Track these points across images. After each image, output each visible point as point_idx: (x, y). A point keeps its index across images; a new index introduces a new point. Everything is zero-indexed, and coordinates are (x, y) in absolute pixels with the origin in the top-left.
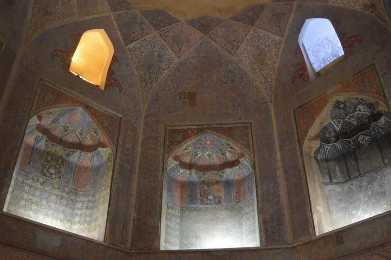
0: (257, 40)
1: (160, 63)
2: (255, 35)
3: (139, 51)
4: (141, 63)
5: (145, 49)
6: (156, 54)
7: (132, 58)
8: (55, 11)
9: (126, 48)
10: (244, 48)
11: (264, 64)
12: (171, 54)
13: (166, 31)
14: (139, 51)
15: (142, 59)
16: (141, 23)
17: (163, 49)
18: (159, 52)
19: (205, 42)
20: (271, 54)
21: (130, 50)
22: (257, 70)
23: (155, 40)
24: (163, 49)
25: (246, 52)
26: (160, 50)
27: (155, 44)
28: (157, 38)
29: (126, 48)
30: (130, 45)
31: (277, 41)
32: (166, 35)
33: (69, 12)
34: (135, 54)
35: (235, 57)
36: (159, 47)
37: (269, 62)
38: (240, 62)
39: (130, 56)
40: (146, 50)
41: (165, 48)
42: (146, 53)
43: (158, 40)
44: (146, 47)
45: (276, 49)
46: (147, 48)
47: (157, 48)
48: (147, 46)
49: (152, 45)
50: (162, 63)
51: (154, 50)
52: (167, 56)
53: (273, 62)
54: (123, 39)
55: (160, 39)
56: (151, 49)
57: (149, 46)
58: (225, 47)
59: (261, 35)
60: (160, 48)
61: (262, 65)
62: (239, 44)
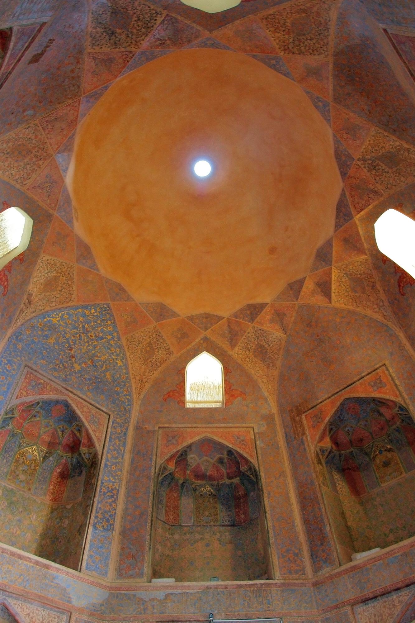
0: (37, 154)
1: (105, 28)
2: (45, 154)
3: (144, 20)
4: (129, 9)
5: (138, 26)
6: (119, 31)
7: (149, 7)
8: (294, 15)
9: (165, 13)
10: (39, 136)
11: (8, 156)
12: (101, 48)
13: (128, 59)
14: (144, 20)
15: (132, 13)
16: (164, 43)
17: (115, 43)
18: (117, 35)
19: (77, 92)
20: (15, 168)
21: (158, 14)
22: (5, 145)
23: (134, 42)
24: (115, 43)
25: (33, 137)
26: (117, 39)
27: (129, 39)
28: (133, 46)
29: (165, 13)
30: (162, 19)
31: (26, 180)
32: (124, 57)
33: (273, 19)
34: (146, 13)
35: (37, 122)
36: (121, 40)
37: (6, 164)
38: (27, 127)
39: (152, 8)
40: (135, 25)
41: (114, 46)
42: (133, 23)
43: (130, 45)
44: (138, 28)
45: (17, 177)
46: (135, 28)
47: (123, 37)
48: (138, 30)
49: (132, 35)
50: (102, 30)
51: (124, 33)
52: (104, 41)
53: (5, 169)
54: (176, 19)
55: (129, 49)
56: (130, 30)
57: (135, 31)
58: (55, 113)
59: (41, 162)
60: (119, 41)
61: (7, 154)
62: (47, 132)
